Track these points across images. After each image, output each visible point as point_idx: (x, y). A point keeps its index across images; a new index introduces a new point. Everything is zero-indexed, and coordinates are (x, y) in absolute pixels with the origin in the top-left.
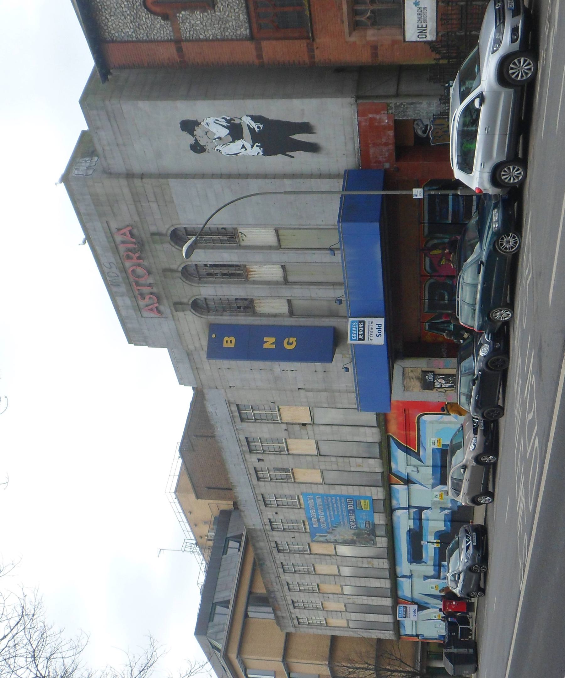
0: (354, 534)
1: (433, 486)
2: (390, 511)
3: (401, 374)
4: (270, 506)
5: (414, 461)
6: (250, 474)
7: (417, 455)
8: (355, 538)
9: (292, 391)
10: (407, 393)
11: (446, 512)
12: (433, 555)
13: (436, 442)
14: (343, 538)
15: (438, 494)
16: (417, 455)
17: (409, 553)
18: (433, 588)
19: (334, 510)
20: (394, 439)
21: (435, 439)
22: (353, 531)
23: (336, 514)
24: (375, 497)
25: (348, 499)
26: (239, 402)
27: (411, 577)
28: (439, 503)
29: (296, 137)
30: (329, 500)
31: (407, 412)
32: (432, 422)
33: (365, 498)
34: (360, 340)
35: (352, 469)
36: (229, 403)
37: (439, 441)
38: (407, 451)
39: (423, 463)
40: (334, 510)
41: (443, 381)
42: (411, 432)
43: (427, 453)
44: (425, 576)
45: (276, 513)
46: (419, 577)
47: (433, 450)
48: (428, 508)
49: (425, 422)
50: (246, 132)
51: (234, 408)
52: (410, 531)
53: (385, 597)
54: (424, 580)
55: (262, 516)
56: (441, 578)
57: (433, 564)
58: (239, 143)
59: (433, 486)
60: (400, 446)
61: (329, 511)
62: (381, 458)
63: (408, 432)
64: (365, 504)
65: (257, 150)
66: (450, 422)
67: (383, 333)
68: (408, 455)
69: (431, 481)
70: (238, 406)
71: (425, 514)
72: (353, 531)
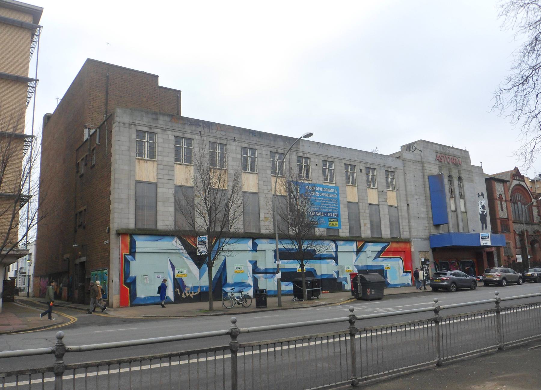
1: (356, 266)
2: (335, 239)
3: (426, 251)
5: (374, 255)
6: (350, 161)
7: (378, 256)
9: (407, 200)
10: (418, 253)
11: (335, 275)
13: (388, 267)
16: (378, 256)
19: (325, 203)
20: (388, 245)
21: (389, 266)
23: (322, 204)
24: (340, 231)
25: (338, 215)
26: (396, 173)
29: (484, 224)
30: (334, 202)
31: (402, 252)
32: (399, 264)
33: (340, 224)
34: (482, 237)
35: (362, 221)
36: (396, 169)
38: (380, 253)
39: (373, 260)
40: (325, 203)
41: (426, 268)
42: (391, 254)
43: (380, 262)
45: (316, 165)
48: (337, 262)
49: (399, 261)
50: (483, 210)
51: (392, 170)
53: (135, 222)
56: (254, 275)
58: (481, 208)
59: (356, 266)
60: (384, 248)
61: (324, 200)
62: (372, 237)
63: (392, 252)
64: (334, 224)
65: (480, 212)
66: (400, 273)
67: (484, 245)
68: (377, 252)
69: (360, 265)
70: (393, 172)
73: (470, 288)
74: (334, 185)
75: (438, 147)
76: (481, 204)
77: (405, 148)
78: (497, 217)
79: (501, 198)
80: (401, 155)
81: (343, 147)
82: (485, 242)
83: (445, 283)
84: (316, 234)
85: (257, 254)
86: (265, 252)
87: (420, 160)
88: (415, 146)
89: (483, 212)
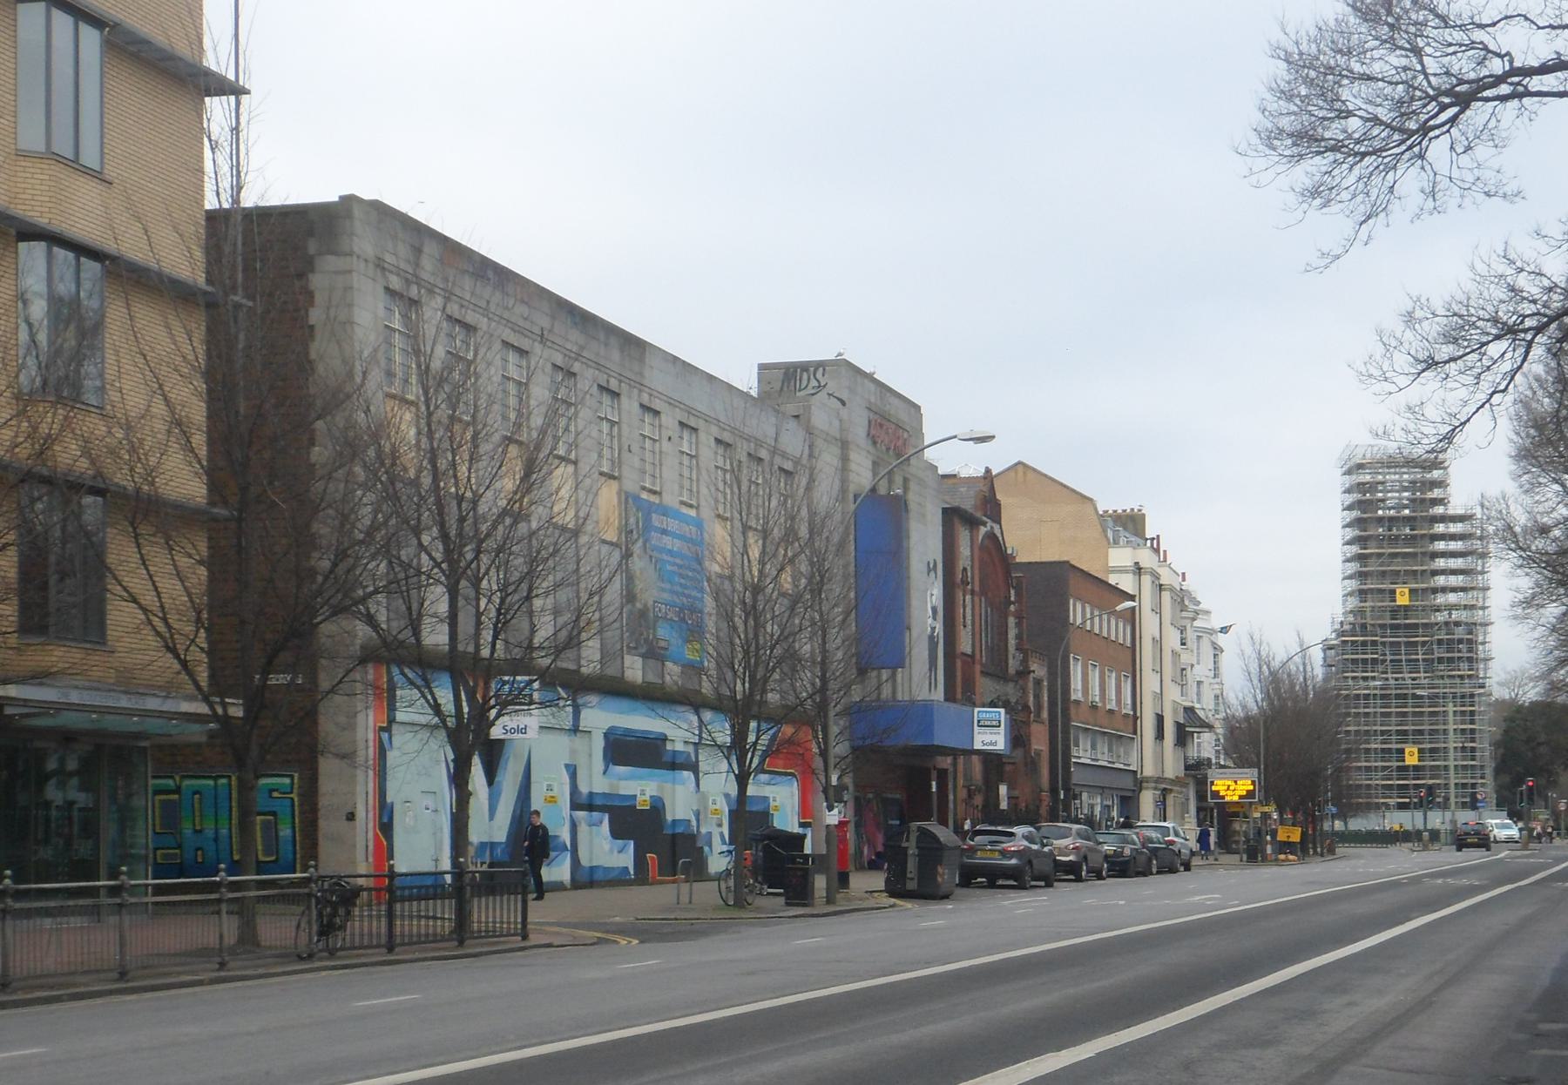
0: (645, 605)
4: (694, 440)
8: (638, 605)
12: (622, 792)
14: (638, 573)
15: (717, 807)
17: (628, 732)
18: (550, 788)
22: (650, 603)
27: (575, 730)
28: (706, 808)
37: (776, 808)
42: (781, 762)
44: (575, 769)
46: (573, 752)
47: (766, 798)
52: (664, 739)
54: (567, 766)
55: (665, 402)
57: (595, 791)
71: (689, 777)
72: (650, 603)
73: (1043, 883)
74: (693, 513)
75: (872, 387)
76: (931, 602)
77: (780, 374)
78: (958, 652)
79: (965, 582)
80: (801, 412)
81: (716, 378)
82: (988, 738)
83: (1014, 861)
84: (626, 675)
85: (578, 741)
86: (590, 739)
87: (838, 436)
88: (819, 375)
89: (933, 629)
